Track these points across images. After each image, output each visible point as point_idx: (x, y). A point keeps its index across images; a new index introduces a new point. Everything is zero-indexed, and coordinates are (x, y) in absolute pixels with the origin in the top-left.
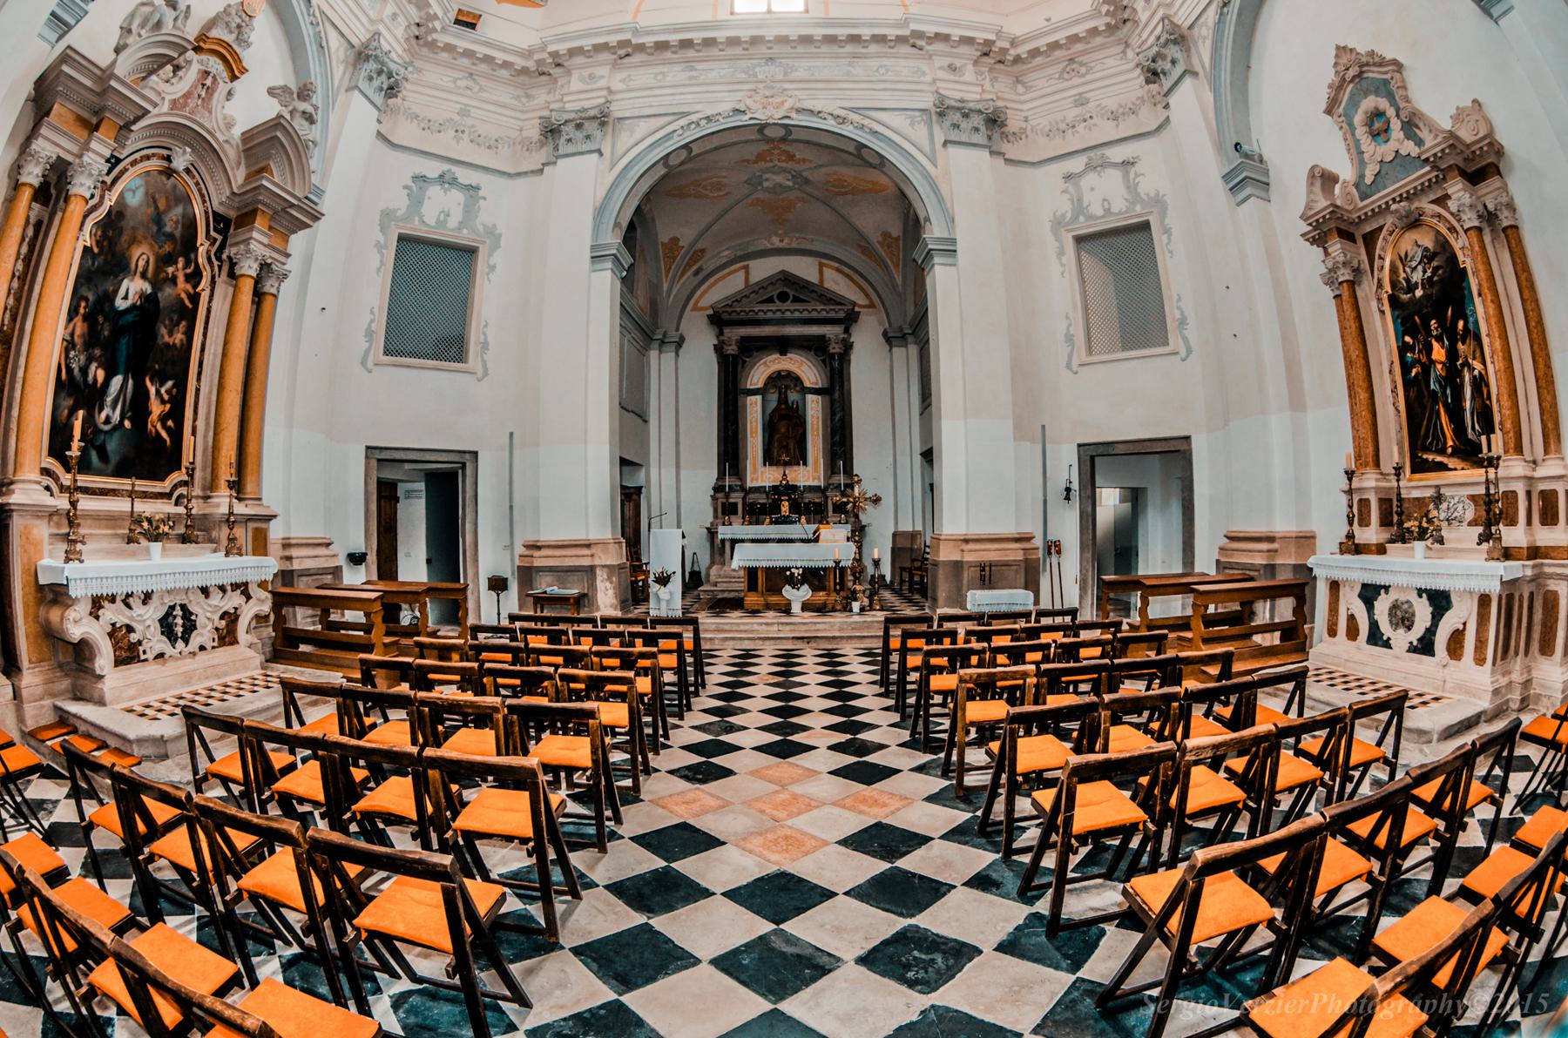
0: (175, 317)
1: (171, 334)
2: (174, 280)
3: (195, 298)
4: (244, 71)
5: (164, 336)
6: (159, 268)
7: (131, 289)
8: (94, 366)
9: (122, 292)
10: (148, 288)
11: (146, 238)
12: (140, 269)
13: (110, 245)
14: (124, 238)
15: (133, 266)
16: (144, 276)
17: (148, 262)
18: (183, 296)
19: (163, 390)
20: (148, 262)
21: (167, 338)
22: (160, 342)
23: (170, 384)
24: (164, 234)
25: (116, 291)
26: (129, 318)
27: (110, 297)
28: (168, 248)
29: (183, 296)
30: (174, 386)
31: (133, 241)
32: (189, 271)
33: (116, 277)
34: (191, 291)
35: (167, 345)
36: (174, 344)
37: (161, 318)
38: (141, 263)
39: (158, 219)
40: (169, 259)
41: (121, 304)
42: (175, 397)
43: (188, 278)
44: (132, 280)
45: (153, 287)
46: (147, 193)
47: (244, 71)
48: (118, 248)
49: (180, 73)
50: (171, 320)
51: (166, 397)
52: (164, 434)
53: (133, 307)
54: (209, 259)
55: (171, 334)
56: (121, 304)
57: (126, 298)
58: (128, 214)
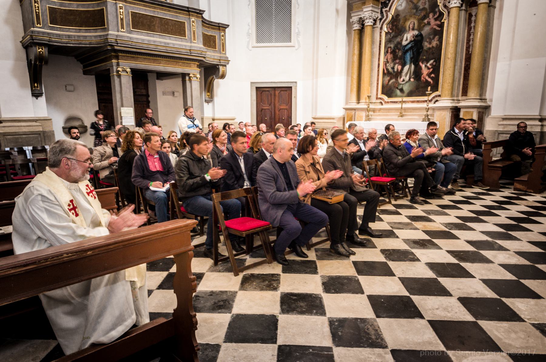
0: (432, 37)
1: (430, 43)
2: (429, 23)
3: (441, 26)
5: (426, 45)
6: (419, 24)
7: (408, 37)
8: (396, 66)
9: (405, 38)
10: (416, 32)
11: (411, 16)
12: (411, 28)
13: (396, 27)
14: (401, 22)
15: (407, 28)
16: (413, 29)
17: (414, 24)
18: (435, 27)
19: (428, 65)
20: (414, 24)
21: (428, 46)
22: (425, 48)
23: (432, 61)
24: (420, 10)
25: (402, 40)
26: (410, 46)
27: (400, 43)
29: (435, 27)
30: (434, 62)
31: (406, 20)
32: (436, 16)
33: (401, 35)
35: (429, 49)
36: (433, 47)
37: (424, 40)
38: (411, 26)
39: (416, 7)
40: (425, 17)
41: (404, 43)
42: (435, 66)
43: (436, 19)
44: (409, 33)
48: (400, 26)
50: (430, 39)
51: (430, 67)
52: (430, 80)
53: (411, 41)
55: (430, 43)
56: (404, 43)
57: (407, 40)
58: (401, 13)
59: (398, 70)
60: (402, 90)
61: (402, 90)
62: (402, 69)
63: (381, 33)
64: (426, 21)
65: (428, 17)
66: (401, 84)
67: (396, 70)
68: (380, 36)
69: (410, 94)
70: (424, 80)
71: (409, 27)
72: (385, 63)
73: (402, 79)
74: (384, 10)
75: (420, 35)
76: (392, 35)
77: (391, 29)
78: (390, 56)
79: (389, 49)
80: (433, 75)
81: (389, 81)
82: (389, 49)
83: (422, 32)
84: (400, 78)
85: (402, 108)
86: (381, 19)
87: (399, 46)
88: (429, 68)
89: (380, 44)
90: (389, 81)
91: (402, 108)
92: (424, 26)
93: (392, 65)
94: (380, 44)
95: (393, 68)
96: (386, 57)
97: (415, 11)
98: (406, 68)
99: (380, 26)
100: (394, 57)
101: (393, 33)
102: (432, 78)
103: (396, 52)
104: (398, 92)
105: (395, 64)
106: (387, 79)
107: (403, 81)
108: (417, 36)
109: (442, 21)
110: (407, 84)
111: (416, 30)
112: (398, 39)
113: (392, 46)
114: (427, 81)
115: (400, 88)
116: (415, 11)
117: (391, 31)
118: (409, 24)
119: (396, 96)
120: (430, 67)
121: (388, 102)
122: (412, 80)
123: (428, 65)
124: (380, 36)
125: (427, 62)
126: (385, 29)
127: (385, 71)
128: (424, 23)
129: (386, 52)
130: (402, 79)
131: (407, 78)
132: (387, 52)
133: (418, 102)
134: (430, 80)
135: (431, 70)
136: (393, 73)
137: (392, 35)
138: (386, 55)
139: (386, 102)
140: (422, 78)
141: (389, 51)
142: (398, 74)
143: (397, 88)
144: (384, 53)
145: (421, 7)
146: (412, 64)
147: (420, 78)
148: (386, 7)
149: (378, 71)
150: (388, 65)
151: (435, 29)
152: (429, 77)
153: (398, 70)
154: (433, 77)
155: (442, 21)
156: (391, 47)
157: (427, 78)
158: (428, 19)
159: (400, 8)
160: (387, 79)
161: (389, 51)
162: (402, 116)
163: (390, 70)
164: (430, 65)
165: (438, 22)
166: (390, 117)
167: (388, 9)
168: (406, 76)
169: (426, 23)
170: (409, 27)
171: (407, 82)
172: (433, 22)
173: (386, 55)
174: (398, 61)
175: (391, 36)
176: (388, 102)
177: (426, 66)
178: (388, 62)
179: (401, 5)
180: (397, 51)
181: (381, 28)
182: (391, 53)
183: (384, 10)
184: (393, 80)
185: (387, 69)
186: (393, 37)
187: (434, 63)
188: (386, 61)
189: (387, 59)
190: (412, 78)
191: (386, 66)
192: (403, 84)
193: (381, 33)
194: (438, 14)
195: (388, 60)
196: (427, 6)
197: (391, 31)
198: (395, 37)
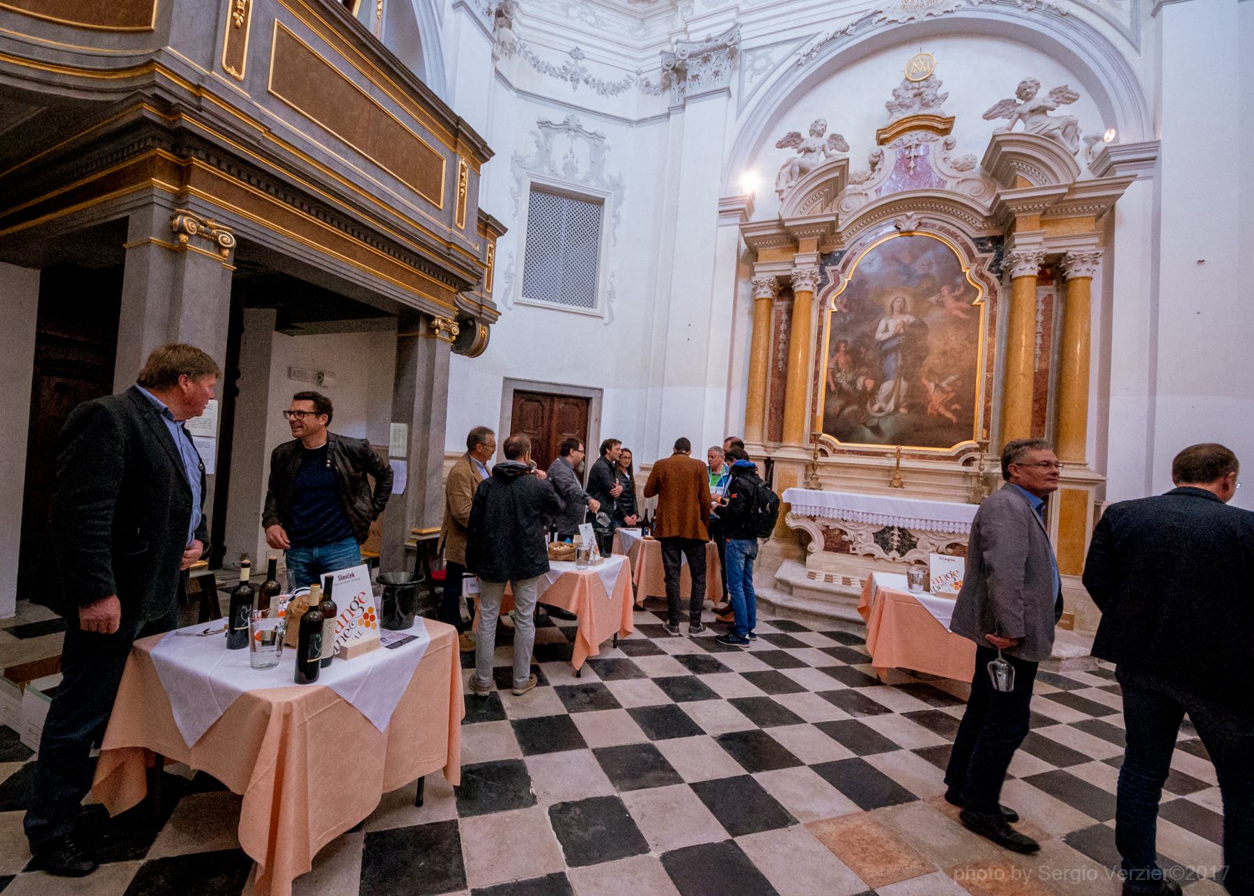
2: (941, 304)
4: (951, 121)
7: (888, 327)
10: (911, 319)
15: (888, 309)
16: (902, 312)
18: (957, 312)
19: (944, 384)
20: (904, 301)
24: (918, 277)
28: (926, 285)
29: (957, 312)
31: (883, 293)
32: (957, 293)
34: (968, 306)
38: (897, 306)
39: (908, 272)
41: (880, 336)
44: (891, 318)
45: (915, 316)
46: (885, 259)
47: (951, 121)
49: (877, 167)
53: (896, 335)
54: (982, 276)
56: (880, 336)
57: (886, 330)
59: (864, 386)
60: (876, 430)
61: (876, 430)
62: (877, 387)
63: (821, 311)
64: (933, 299)
65: (939, 291)
66: (873, 417)
67: (859, 386)
68: (821, 317)
69: (899, 440)
70: (935, 413)
71: (892, 307)
72: (830, 371)
73: (876, 407)
74: (828, 269)
75: (922, 325)
76: (848, 318)
77: (845, 306)
78: (842, 358)
79: (842, 345)
80: (956, 406)
81: (842, 408)
82: (842, 345)
83: (925, 320)
84: (873, 404)
85: (898, 467)
86: (820, 286)
87: (867, 341)
88: (944, 391)
89: (820, 333)
90: (842, 408)
91: (898, 467)
92: (929, 308)
93: (850, 377)
94: (820, 333)
95: (853, 383)
96: (834, 360)
97: (905, 278)
98: (887, 387)
99: (819, 298)
100: (854, 362)
101: (853, 315)
102: (954, 412)
103: (859, 352)
104: (868, 433)
105: (857, 376)
106: (837, 403)
107: (881, 410)
108: (912, 325)
109: (975, 303)
110: (890, 420)
111: (910, 314)
112: (865, 328)
113: (849, 339)
114: (940, 415)
115: (872, 425)
116: (905, 278)
117: (845, 311)
118: (893, 299)
119: (862, 441)
120: (949, 389)
121: (842, 452)
122: (902, 410)
123: (944, 384)
124: (821, 317)
125: (943, 379)
126: (832, 306)
127: (833, 387)
128: (929, 302)
129: (834, 351)
130: (876, 407)
131: (891, 406)
132: (837, 350)
133: (922, 457)
134: (949, 415)
135: (952, 395)
136: (852, 392)
137: (848, 318)
138: (833, 356)
139: (835, 451)
140: (929, 410)
141: (842, 349)
142: (868, 396)
143: (865, 424)
144: (830, 351)
145: (920, 272)
146: (902, 379)
147: (924, 408)
148: (836, 262)
149: (816, 385)
150: (838, 375)
151: (956, 316)
152: (948, 409)
153: (864, 386)
154: (956, 409)
155: (975, 303)
156: (846, 342)
157: (942, 410)
158: (938, 295)
159: (867, 270)
160: (837, 403)
161: (842, 349)
162: (901, 485)
163: (845, 385)
164: (948, 384)
165: (964, 305)
166: (857, 484)
167: (839, 267)
168: (887, 399)
169: (934, 303)
170: (892, 307)
171: (889, 414)
172: (950, 302)
173: (833, 356)
174: (864, 370)
175: (845, 320)
176: (842, 452)
177: (937, 386)
178: (839, 371)
179: (870, 264)
180: (863, 350)
181: (823, 302)
182: (846, 353)
183: (828, 269)
184: (855, 407)
185: (837, 384)
186: (849, 323)
187: (960, 383)
188: (834, 367)
189: (837, 364)
190: (904, 407)
191: (833, 374)
192: (879, 418)
193: (821, 311)
194: (962, 289)
195: (840, 366)
196: (934, 271)
197: (845, 311)
198: (857, 322)
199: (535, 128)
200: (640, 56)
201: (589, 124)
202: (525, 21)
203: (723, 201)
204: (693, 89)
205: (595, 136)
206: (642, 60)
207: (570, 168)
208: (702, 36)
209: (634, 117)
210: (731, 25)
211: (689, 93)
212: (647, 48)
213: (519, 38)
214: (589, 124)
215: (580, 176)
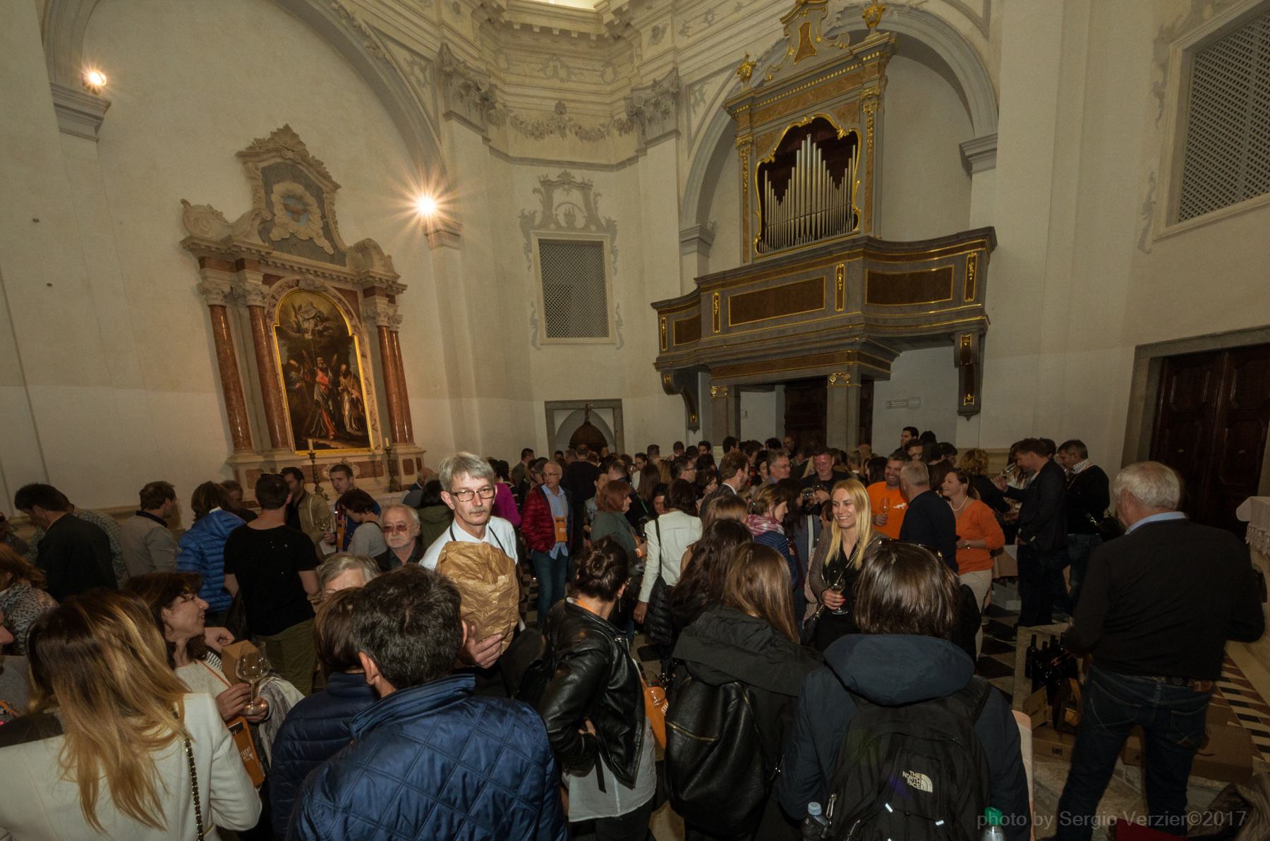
199: (538, 186)
200: (608, 100)
201: (578, 175)
202: (507, 89)
203: (682, 234)
204: (654, 131)
205: (585, 187)
206: (612, 103)
207: (570, 217)
208: (648, 81)
209: (614, 162)
210: (670, 67)
211: (650, 136)
212: (612, 93)
213: (505, 106)
214: (578, 175)
215: (580, 222)
